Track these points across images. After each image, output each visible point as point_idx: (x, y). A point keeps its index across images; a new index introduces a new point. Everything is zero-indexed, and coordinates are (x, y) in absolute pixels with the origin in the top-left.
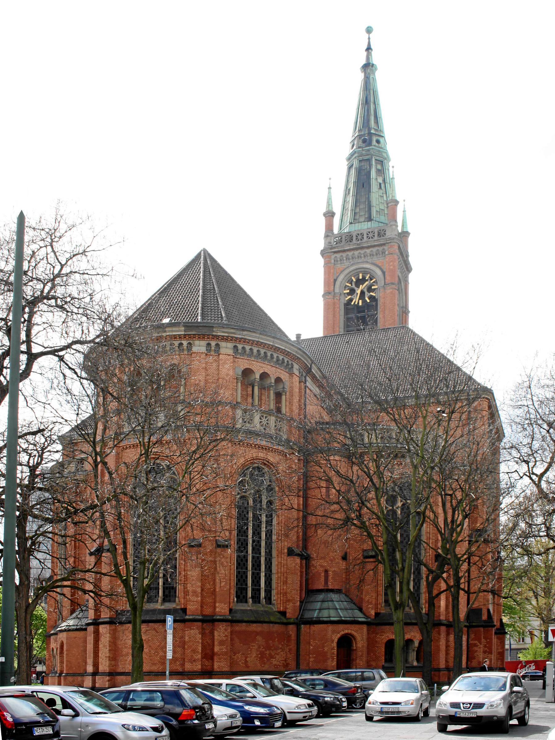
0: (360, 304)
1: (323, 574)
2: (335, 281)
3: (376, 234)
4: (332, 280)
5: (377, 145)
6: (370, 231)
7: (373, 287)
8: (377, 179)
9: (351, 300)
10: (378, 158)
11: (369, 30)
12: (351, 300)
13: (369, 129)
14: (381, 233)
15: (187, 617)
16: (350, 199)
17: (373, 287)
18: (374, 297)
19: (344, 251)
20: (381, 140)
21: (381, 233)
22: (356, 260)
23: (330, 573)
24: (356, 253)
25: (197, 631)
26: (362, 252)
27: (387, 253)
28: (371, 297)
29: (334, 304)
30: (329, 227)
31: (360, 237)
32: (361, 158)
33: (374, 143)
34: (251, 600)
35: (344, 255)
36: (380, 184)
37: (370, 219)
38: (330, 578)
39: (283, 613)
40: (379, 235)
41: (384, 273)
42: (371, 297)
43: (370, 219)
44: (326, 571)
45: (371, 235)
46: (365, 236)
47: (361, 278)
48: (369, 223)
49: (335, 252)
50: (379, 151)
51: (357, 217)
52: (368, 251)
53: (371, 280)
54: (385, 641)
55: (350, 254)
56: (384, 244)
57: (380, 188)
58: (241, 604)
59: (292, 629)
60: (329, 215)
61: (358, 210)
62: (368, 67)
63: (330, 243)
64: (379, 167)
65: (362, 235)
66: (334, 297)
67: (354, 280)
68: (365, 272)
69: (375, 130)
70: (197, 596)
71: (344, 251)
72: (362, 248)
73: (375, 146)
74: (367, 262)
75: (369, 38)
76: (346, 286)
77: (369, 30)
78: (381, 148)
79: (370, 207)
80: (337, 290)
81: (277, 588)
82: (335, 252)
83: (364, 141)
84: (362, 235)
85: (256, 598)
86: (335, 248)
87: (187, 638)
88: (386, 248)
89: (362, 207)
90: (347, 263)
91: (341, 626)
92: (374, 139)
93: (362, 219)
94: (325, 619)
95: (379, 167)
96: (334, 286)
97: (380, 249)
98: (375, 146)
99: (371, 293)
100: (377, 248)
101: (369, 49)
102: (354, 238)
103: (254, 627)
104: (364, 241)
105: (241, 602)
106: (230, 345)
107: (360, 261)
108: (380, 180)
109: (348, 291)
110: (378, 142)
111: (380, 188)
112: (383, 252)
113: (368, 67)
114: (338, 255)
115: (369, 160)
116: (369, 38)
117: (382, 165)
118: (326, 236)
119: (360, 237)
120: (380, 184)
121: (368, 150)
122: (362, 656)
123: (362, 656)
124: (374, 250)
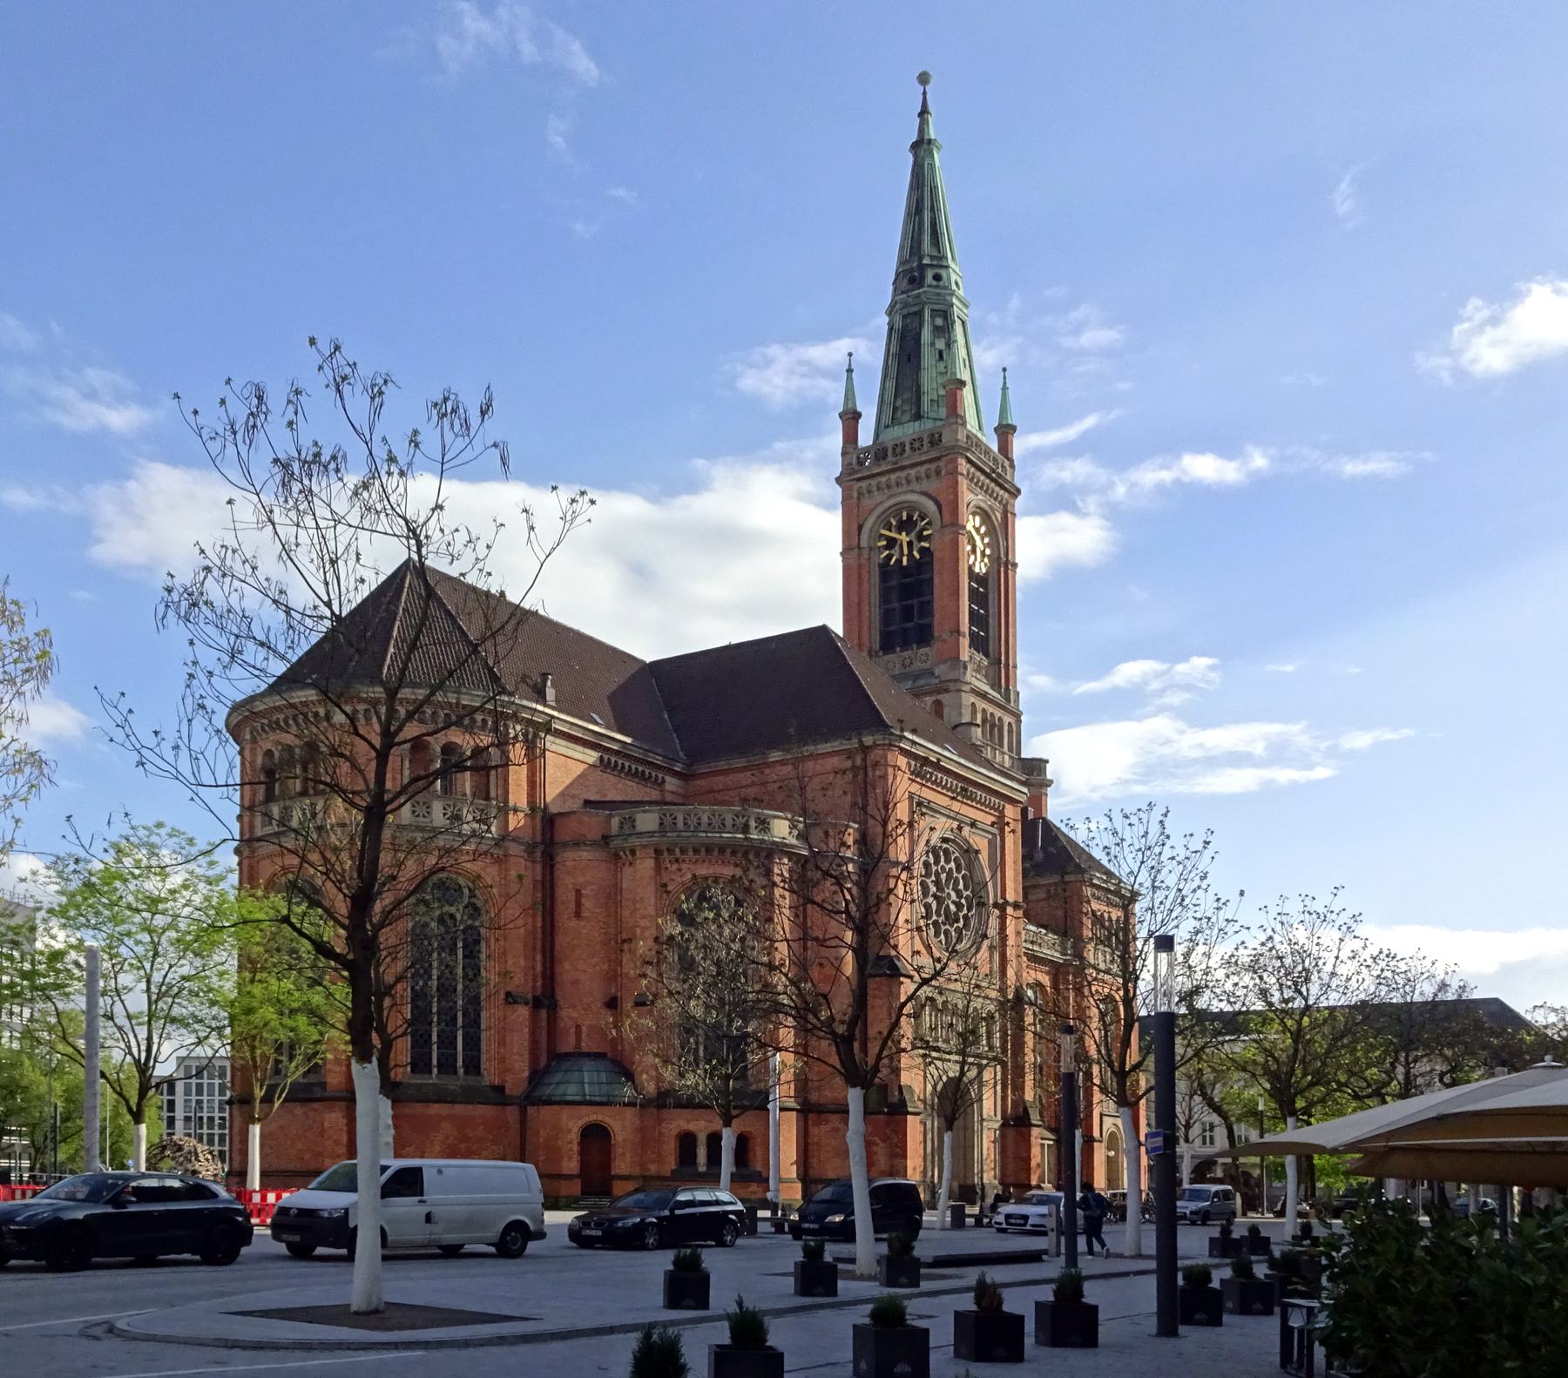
0: (905, 562)
1: (573, 1030)
2: (860, 528)
3: (926, 441)
4: (856, 527)
5: (934, 283)
6: (915, 437)
7: (925, 533)
8: (933, 344)
9: (889, 557)
10: (937, 307)
11: (924, 79)
12: (889, 557)
14: (935, 440)
15: (326, 1094)
16: (891, 385)
17: (925, 533)
18: (928, 549)
19: (874, 476)
20: (943, 273)
21: (935, 440)
22: (895, 490)
23: (584, 1029)
24: (893, 477)
25: (339, 1115)
26: (903, 474)
27: (943, 472)
28: (922, 551)
29: (860, 566)
30: (850, 436)
31: (898, 450)
32: (905, 311)
33: (929, 279)
34: (435, 1071)
35: (874, 482)
36: (941, 353)
37: (918, 416)
38: (584, 1035)
39: (500, 1089)
40: (931, 443)
42: (922, 551)
44: (578, 1027)
45: (917, 445)
46: (907, 448)
47: (904, 518)
48: (917, 423)
49: (859, 480)
50: (939, 294)
51: (899, 414)
52: (913, 472)
53: (923, 519)
54: (674, 1132)
55: (883, 479)
56: (938, 459)
57: (941, 357)
58: (419, 1076)
59: (512, 1113)
60: (851, 418)
61: (899, 403)
62: (922, 146)
63: (850, 464)
64: (939, 322)
65: (903, 445)
66: (859, 555)
67: (894, 523)
68: (911, 508)
69: (932, 258)
70: (340, 1065)
71: (874, 476)
72: (903, 468)
73: (930, 286)
74: (913, 491)
75: (924, 93)
76: (882, 535)
77: (924, 79)
78: (945, 288)
80: (864, 544)
81: (488, 1051)
82: (859, 480)
83: (912, 281)
84: (903, 445)
85: (447, 1066)
86: (857, 472)
87: (326, 1124)
88: (941, 464)
89: (905, 396)
90: (878, 497)
91: (585, 1109)
92: (930, 274)
93: (907, 417)
94: (557, 1098)
95: (939, 322)
96: (859, 535)
97: (933, 466)
98: (930, 286)
99: (923, 544)
100: (926, 467)
101: (924, 112)
102: (890, 452)
103: (436, 1109)
104: (905, 455)
105: (422, 1072)
107: (900, 490)
108: (940, 344)
109: (884, 543)
110: (937, 278)
111: (941, 357)
112: (938, 473)
113: (922, 146)
114: (864, 484)
115: (920, 314)
116: (924, 93)
117: (945, 318)
118: (844, 454)
120: (941, 353)
121: (918, 296)
122: (624, 1154)
123: (624, 1154)
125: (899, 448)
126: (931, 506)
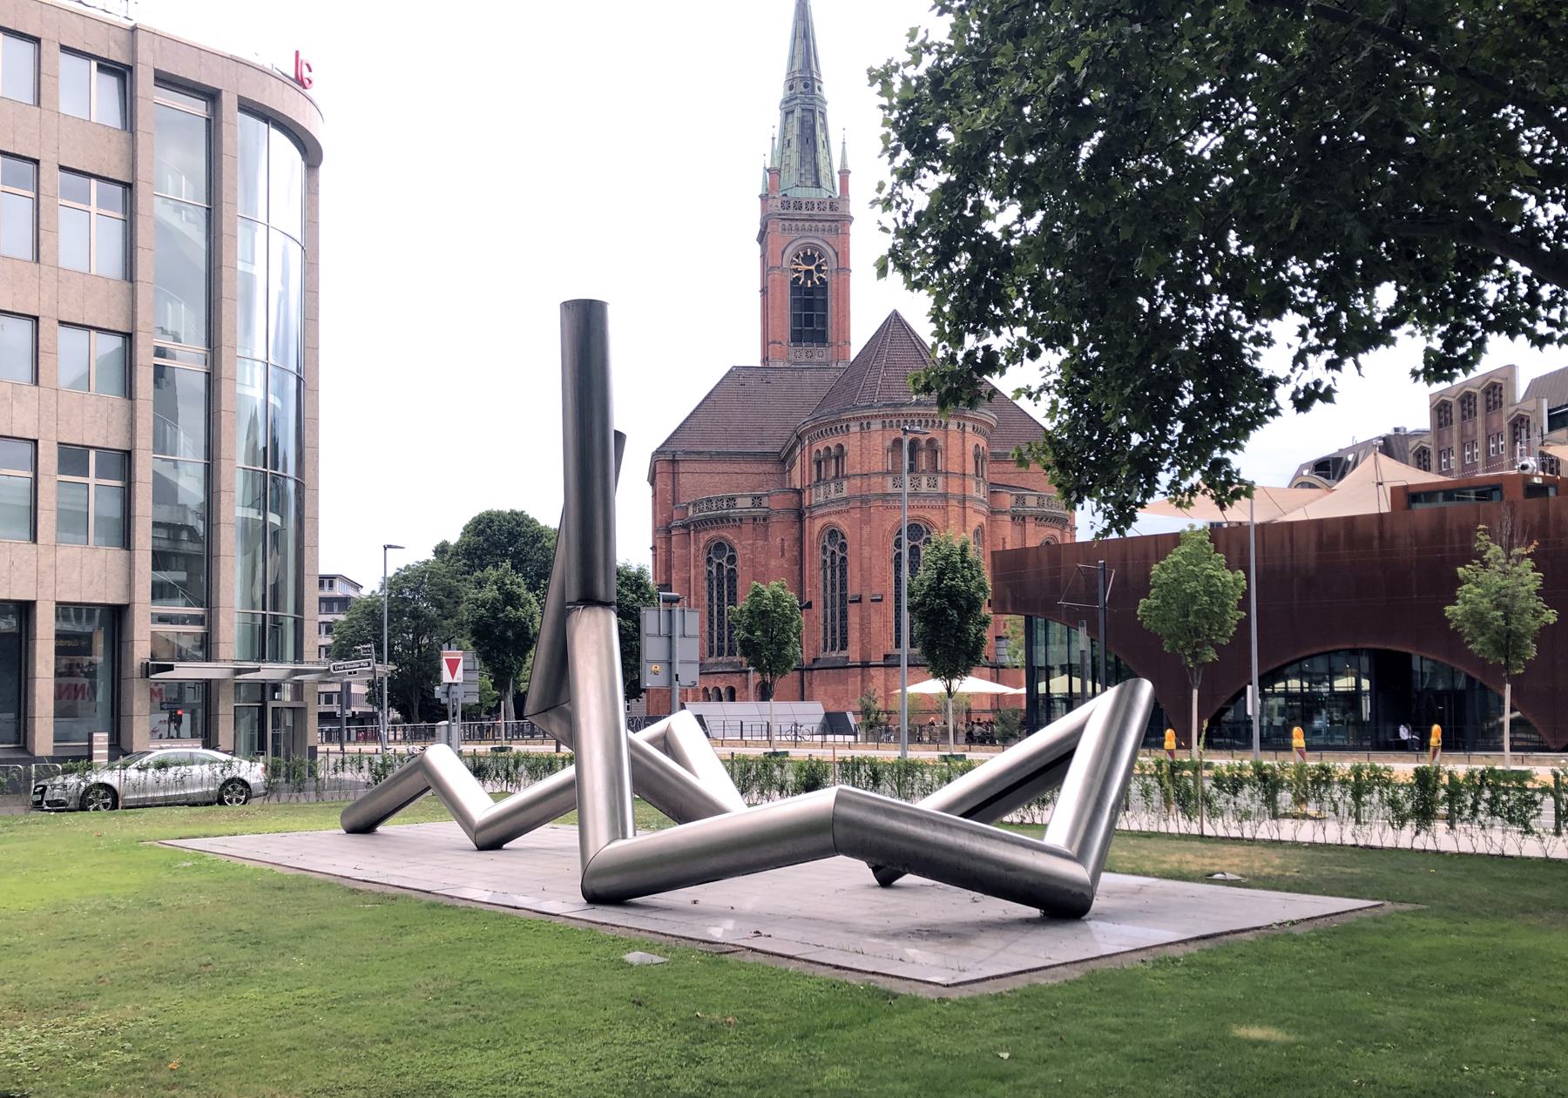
2: (783, 253)
13: (811, 73)
22: (807, 234)
24: (807, 224)
26: (814, 224)
31: (810, 206)
35: (793, 224)
41: (837, 254)
43: (818, 185)
52: (820, 225)
55: (800, 224)
68: (815, 248)
79: (817, 171)
89: (807, 167)
90: (795, 235)
92: (817, 84)
93: (809, 183)
97: (833, 225)
106: (879, 421)
110: (819, 89)
114: (787, 223)
115: (812, 111)
119: (810, 206)
124: (827, 224)
125: (810, 205)
126: (831, 253)
